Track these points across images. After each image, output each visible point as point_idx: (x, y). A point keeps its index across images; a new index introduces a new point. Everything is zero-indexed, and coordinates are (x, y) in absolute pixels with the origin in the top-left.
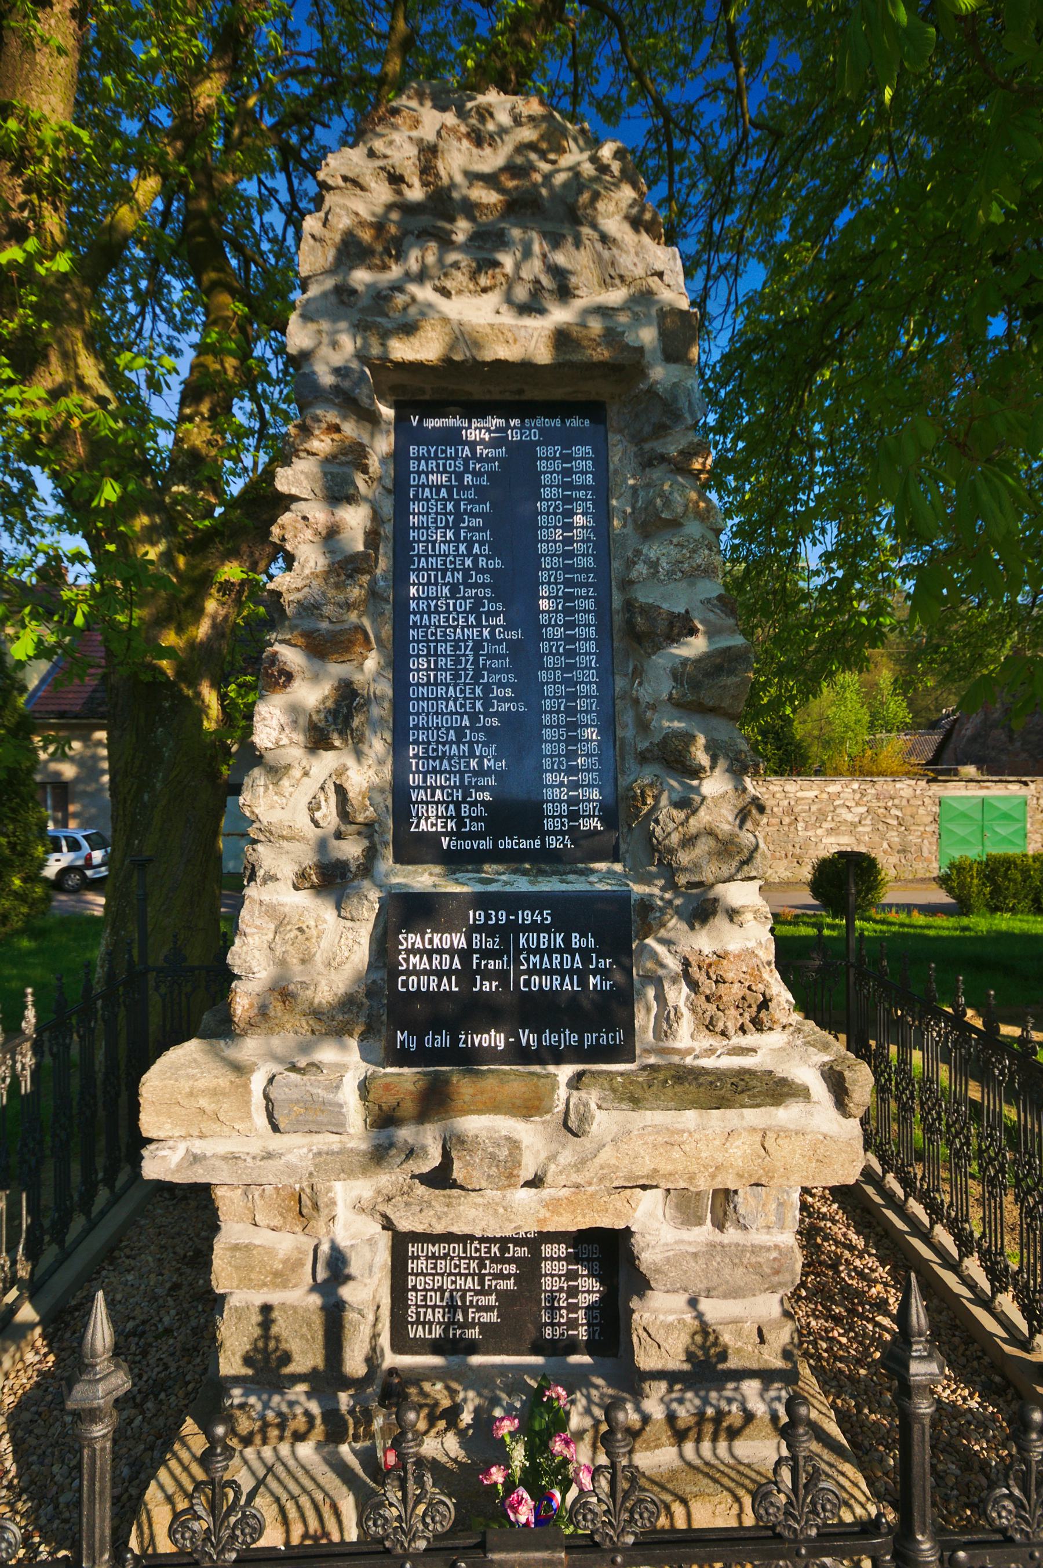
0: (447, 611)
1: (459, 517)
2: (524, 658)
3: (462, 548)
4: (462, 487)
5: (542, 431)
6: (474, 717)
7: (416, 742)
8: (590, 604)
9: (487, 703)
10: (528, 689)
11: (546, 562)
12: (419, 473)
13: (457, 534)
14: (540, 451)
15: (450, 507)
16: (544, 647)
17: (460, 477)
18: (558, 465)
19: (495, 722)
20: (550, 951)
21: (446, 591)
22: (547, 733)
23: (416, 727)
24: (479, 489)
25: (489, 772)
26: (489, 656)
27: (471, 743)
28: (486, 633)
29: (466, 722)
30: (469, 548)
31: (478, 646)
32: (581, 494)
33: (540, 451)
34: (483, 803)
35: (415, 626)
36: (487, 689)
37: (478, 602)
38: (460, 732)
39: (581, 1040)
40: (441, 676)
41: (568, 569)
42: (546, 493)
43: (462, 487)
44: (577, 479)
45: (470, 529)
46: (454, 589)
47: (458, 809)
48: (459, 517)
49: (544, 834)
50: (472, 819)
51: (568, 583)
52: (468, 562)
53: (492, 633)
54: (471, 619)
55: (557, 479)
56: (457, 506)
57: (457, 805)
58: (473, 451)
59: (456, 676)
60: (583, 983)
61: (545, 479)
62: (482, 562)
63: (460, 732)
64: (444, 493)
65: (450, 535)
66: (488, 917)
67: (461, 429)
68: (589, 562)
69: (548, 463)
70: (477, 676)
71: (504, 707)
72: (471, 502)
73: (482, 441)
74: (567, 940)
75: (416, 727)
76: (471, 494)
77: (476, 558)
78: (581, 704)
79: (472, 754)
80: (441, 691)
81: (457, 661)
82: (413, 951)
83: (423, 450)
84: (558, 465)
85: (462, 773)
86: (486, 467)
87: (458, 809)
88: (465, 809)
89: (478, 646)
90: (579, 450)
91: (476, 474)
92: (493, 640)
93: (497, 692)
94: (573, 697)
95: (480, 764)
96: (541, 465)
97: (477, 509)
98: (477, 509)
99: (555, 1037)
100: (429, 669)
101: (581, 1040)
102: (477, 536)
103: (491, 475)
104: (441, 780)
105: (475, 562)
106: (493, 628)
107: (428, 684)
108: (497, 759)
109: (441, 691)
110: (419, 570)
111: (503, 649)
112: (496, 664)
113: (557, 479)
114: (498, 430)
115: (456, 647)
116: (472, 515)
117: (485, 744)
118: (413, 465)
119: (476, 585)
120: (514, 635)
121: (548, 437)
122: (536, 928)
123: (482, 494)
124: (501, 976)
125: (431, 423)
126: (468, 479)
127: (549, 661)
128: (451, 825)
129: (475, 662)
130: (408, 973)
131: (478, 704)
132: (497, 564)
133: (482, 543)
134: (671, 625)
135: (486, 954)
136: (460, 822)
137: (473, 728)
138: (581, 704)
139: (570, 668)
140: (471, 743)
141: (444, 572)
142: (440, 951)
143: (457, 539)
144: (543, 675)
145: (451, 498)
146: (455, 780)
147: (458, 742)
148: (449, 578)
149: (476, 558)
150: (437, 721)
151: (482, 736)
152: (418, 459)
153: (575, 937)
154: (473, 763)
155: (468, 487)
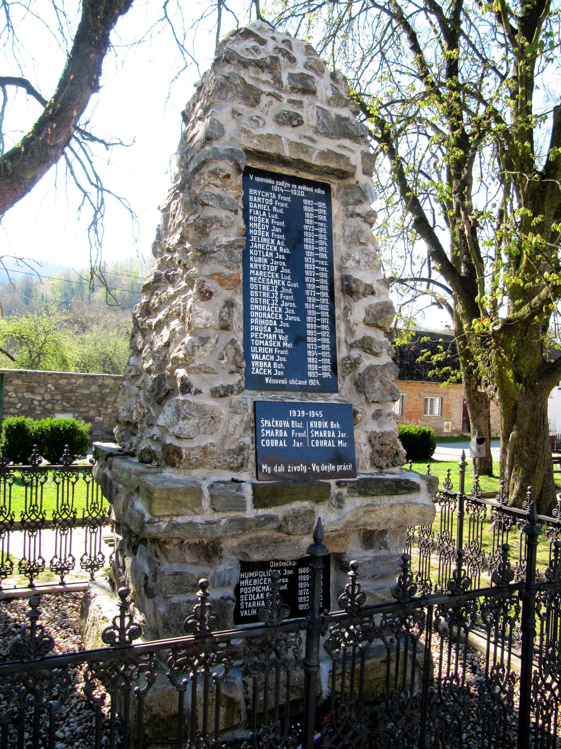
0: (266, 270)
2: (299, 296)
3: (273, 241)
4: (272, 213)
6: (278, 322)
7: (254, 331)
9: (284, 316)
10: (301, 311)
12: (254, 202)
13: (270, 234)
14: (305, 201)
15: (267, 221)
16: (307, 292)
17: (271, 207)
19: (287, 325)
20: (322, 429)
21: (266, 260)
23: (254, 324)
24: (279, 214)
25: (285, 348)
26: (285, 294)
27: (277, 334)
28: (283, 283)
29: (275, 324)
30: (276, 242)
32: (322, 224)
33: (305, 201)
34: (283, 362)
35: (252, 276)
36: (284, 309)
37: (279, 268)
38: (273, 328)
39: (336, 468)
40: (264, 301)
41: (317, 258)
42: (307, 221)
43: (272, 213)
45: (276, 233)
46: (269, 261)
47: (272, 365)
49: (308, 378)
50: (279, 370)
52: (275, 248)
53: (286, 283)
54: (277, 275)
55: (312, 216)
56: (270, 221)
57: (272, 362)
58: (277, 196)
59: (271, 302)
60: (336, 443)
62: (281, 249)
64: (264, 214)
65: (267, 234)
66: (297, 413)
67: (271, 185)
71: (291, 318)
72: (276, 220)
73: (280, 192)
74: (329, 425)
75: (254, 324)
77: (278, 247)
79: (278, 339)
80: (264, 308)
81: (271, 295)
82: (267, 428)
83: (255, 192)
85: (274, 348)
86: (282, 205)
87: (272, 365)
88: (275, 364)
89: (280, 289)
91: (279, 207)
95: (281, 344)
97: (278, 224)
98: (278, 224)
99: (326, 467)
100: (258, 297)
101: (336, 468)
102: (279, 237)
103: (285, 209)
104: (265, 350)
105: (278, 249)
106: (286, 281)
107: (258, 304)
108: (289, 342)
109: (264, 308)
110: (254, 249)
111: (290, 291)
112: (287, 298)
114: (287, 188)
115: (271, 288)
116: (276, 226)
117: (283, 335)
118: (251, 198)
119: (278, 260)
120: (296, 285)
121: (308, 196)
122: (316, 419)
124: (303, 440)
126: (275, 209)
127: (309, 299)
128: (270, 371)
129: (279, 296)
130: (266, 438)
131: (280, 316)
132: (287, 251)
133: (281, 240)
134: (366, 289)
135: (298, 430)
136: (273, 371)
137: (278, 327)
139: (318, 303)
140: (277, 334)
141: (265, 251)
142: (279, 428)
143: (270, 237)
144: (307, 305)
145: (267, 217)
146: (271, 350)
147: (272, 333)
148: (267, 255)
149: (278, 247)
151: (282, 331)
152: (253, 196)
154: (279, 343)
155: (275, 213)
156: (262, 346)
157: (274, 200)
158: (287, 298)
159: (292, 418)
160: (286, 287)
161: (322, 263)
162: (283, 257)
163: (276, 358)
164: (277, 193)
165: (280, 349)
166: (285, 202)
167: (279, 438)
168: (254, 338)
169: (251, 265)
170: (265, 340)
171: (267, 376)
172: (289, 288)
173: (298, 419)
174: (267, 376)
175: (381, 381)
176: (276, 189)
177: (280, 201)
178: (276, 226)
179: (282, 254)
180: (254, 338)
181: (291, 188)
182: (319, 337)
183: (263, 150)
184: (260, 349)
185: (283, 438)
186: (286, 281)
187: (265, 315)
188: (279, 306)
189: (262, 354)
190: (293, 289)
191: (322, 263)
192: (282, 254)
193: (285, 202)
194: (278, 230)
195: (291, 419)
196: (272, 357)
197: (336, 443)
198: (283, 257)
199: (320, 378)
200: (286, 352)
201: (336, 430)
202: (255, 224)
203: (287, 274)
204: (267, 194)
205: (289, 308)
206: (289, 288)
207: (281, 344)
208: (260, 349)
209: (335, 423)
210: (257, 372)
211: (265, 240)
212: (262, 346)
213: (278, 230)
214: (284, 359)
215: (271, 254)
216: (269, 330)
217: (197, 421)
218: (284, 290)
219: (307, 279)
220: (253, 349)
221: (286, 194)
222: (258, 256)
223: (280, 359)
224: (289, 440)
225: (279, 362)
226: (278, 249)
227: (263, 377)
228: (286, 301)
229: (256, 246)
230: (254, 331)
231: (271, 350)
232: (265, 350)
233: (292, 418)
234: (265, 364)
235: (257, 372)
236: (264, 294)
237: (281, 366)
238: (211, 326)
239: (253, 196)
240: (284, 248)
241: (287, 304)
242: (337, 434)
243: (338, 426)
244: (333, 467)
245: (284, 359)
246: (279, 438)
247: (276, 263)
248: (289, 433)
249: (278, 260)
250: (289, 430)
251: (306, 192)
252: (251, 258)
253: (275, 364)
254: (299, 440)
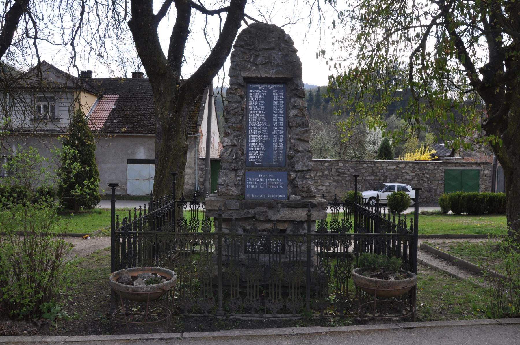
1: (258, 104)
2: (270, 130)
4: (259, 98)
5: (274, 87)
6: (261, 141)
8: (282, 120)
9: (263, 138)
10: (270, 135)
11: (274, 112)
14: (274, 91)
16: (274, 128)
17: (259, 96)
18: (277, 94)
22: (274, 144)
24: (262, 98)
31: (262, 127)
33: (274, 91)
36: (263, 135)
37: (262, 120)
38: (258, 143)
41: (278, 113)
42: (275, 99)
43: (259, 98)
44: (280, 97)
46: (257, 117)
48: (258, 104)
49: (273, 162)
51: (278, 116)
55: (277, 97)
60: (279, 187)
61: (274, 97)
63: (258, 143)
68: (282, 112)
69: (275, 94)
70: (261, 133)
76: (261, 99)
78: (281, 138)
79: (260, 147)
82: (249, 181)
84: (277, 94)
89: (262, 127)
90: (281, 91)
91: (262, 95)
92: (264, 127)
93: (265, 136)
94: (279, 137)
96: (274, 94)
97: (262, 102)
98: (262, 102)
104: (255, 152)
111: (266, 128)
113: (277, 97)
118: (250, 94)
121: (275, 89)
123: (263, 99)
124: (265, 185)
125: (253, 86)
126: (260, 96)
127: (275, 131)
130: (249, 185)
132: (265, 112)
135: (262, 182)
137: (261, 143)
138: (281, 138)
139: (278, 132)
142: (254, 181)
144: (273, 133)
146: (257, 152)
147: (258, 145)
150: (254, 141)
153: (277, 179)
160: (264, 127)
164: (261, 90)
166: (264, 93)
176: (261, 88)
177: (263, 93)
182: (279, 145)
183: (250, 76)
185: (256, 185)
193: (264, 93)
194: (261, 105)
195: (259, 178)
196: (258, 155)
197: (279, 187)
199: (279, 162)
201: (279, 182)
213: (261, 105)
219: (274, 123)
221: (265, 90)
223: (261, 155)
224: (258, 185)
227: (254, 162)
232: (255, 152)
237: (261, 157)
238: (229, 145)
242: (279, 183)
250: (259, 182)
251: (274, 87)
253: (259, 157)
254: (262, 185)
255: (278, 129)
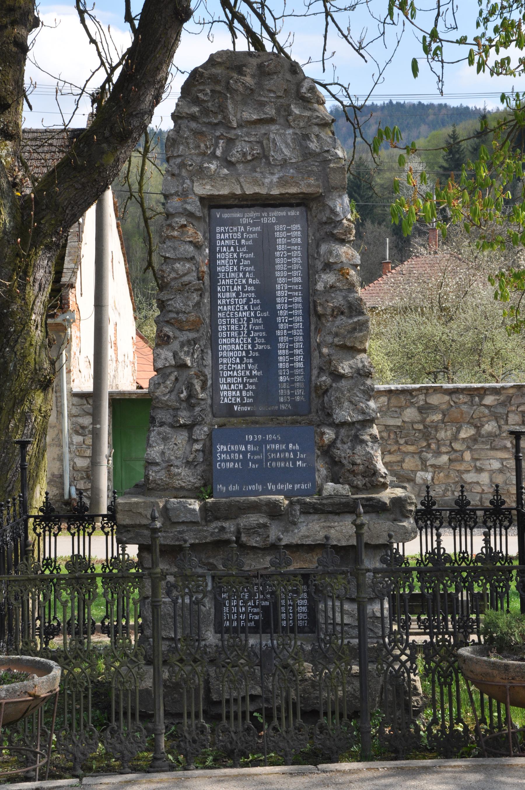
0: (235, 304)
1: (239, 261)
2: (270, 326)
3: (241, 275)
4: (241, 246)
5: (277, 218)
6: (247, 352)
7: (222, 363)
8: (300, 299)
9: (253, 346)
10: (271, 338)
11: (280, 280)
12: (221, 240)
13: (238, 268)
14: (277, 228)
15: (235, 255)
16: (279, 319)
17: (239, 241)
18: (284, 234)
19: (257, 354)
20: (280, 451)
21: (234, 295)
22: (281, 359)
23: (222, 357)
24: (248, 246)
25: (255, 376)
26: (254, 324)
27: (246, 364)
28: (252, 314)
29: (244, 354)
30: (244, 275)
31: (249, 320)
32: (295, 248)
33: (277, 228)
34: (252, 390)
35: (220, 311)
36: (253, 339)
37: (249, 300)
38: (241, 358)
39: (293, 487)
40: (233, 334)
41: (289, 283)
42: (279, 247)
43: (241, 246)
44: (293, 241)
45: (244, 266)
46: (238, 294)
47: (241, 393)
48: (239, 261)
49: (279, 403)
50: (247, 397)
51: (289, 290)
52: (244, 281)
53: (255, 314)
54: (246, 307)
55: (284, 241)
56: (238, 255)
57: (241, 391)
58: (245, 229)
59: (239, 334)
60: (294, 464)
61: (279, 241)
62: (250, 281)
63: (241, 358)
64: (232, 249)
65: (235, 268)
66: (254, 438)
67: (239, 218)
68: (299, 280)
69: (280, 236)
70: (249, 333)
71: (261, 347)
72: (245, 253)
73: (249, 224)
74: (287, 447)
75: (222, 357)
76: (245, 249)
77: (247, 279)
78: (296, 345)
79: (247, 368)
80: (233, 340)
81: (240, 327)
82: (222, 452)
83: (222, 229)
84: (284, 234)
85: (242, 377)
86: (251, 236)
87: (241, 393)
88: (244, 393)
90: (295, 227)
91: (247, 239)
92: (256, 317)
93: (257, 340)
94: (292, 342)
95: (251, 373)
96: (277, 234)
97: (247, 256)
98: (247, 256)
99: (282, 487)
100: (227, 331)
101: (293, 487)
102: (248, 269)
103: (254, 240)
104: (234, 380)
105: (247, 281)
106: (255, 312)
107: (227, 337)
108: (258, 371)
109: (233, 340)
110: (221, 285)
111: (260, 321)
112: (257, 328)
113: (284, 241)
114: (257, 218)
115: (239, 321)
116: (245, 259)
117: (253, 364)
118: (218, 236)
119: (247, 292)
120: (266, 314)
122: (274, 442)
123: (250, 249)
124: (259, 462)
125: (226, 216)
126: (243, 242)
127: (281, 326)
128: (238, 400)
129: (248, 327)
130: (221, 461)
131: (250, 347)
132: (257, 282)
133: (250, 272)
134: (333, 311)
135: (253, 453)
136: (242, 398)
137: (247, 357)
138: (296, 345)
139: (291, 329)
140: (246, 364)
141: (233, 286)
142: (234, 452)
143: (239, 270)
145: (235, 251)
146: (239, 380)
147: (241, 363)
148: (235, 289)
149: (247, 279)
150: (231, 354)
151: (251, 361)
152: (220, 233)
153: (291, 446)
154: (248, 373)
155: (243, 246)
156: (230, 376)
157: (242, 233)
158: (257, 328)
159: (249, 442)
160: (256, 317)
161: (296, 287)
162: (253, 288)
163: (245, 386)
164: (245, 226)
165: (249, 377)
166: (254, 233)
167: (234, 461)
168: (222, 370)
169: (219, 302)
170: (233, 371)
171: (236, 404)
172: (259, 318)
173: (253, 443)
174: (236, 404)
175: (351, 402)
176: (245, 221)
177: (249, 233)
178: (245, 259)
179: (251, 285)
180: (222, 370)
181: (262, 217)
182: (292, 362)
183: (217, 193)
184: (229, 380)
185: (238, 461)
186: (255, 312)
187: (233, 347)
188: (249, 337)
189: (230, 384)
190: (263, 318)
191: (296, 287)
192: (251, 285)
193: (254, 233)
194: (246, 262)
195: (246, 444)
196: (241, 387)
197: (294, 464)
198: (253, 288)
199: (293, 403)
200: (256, 380)
201: (295, 452)
202: (223, 261)
203: (257, 305)
204: (235, 229)
205: (259, 337)
206: (259, 318)
207: (251, 373)
208: (229, 380)
209: (294, 444)
210: (226, 401)
211: (233, 275)
212: (230, 376)
213: (246, 262)
214: (254, 387)
215: (240, 288)
216: (238, 360)
217: (162, 447)
218: (253, 321)
219: (278, 307)
220: (222, 380)
221: (254, 225)
222: (226, 291)
223: (249, 387)
224: (245, 462)
225: (248, 391)
226: (247, 281)
227: (232, 405)
228: (255, 331)
229: (223, 282)
230: (222, 363)
231: (239, 380)
232: (234, 380)
233: (249, 442)
234: (234, 393)
235: (226, 401)
236: (233, 328)
237: (250, 393)
238: (171, 366)
239: (220, 233)
240: (253, 279)
241: (257, 334)
242: (295, 455)
243: (297, 447)
244: (291, 486)
245: (254, 387)
246: (234, 461)
247: (245, 295)
248: (245, 456)
249: (247, 292)
250: (245, 453)
251: (277, 218)
252: (219, 295)
253: (244, 393)
254: (254, 462)
255: (291, 322)
